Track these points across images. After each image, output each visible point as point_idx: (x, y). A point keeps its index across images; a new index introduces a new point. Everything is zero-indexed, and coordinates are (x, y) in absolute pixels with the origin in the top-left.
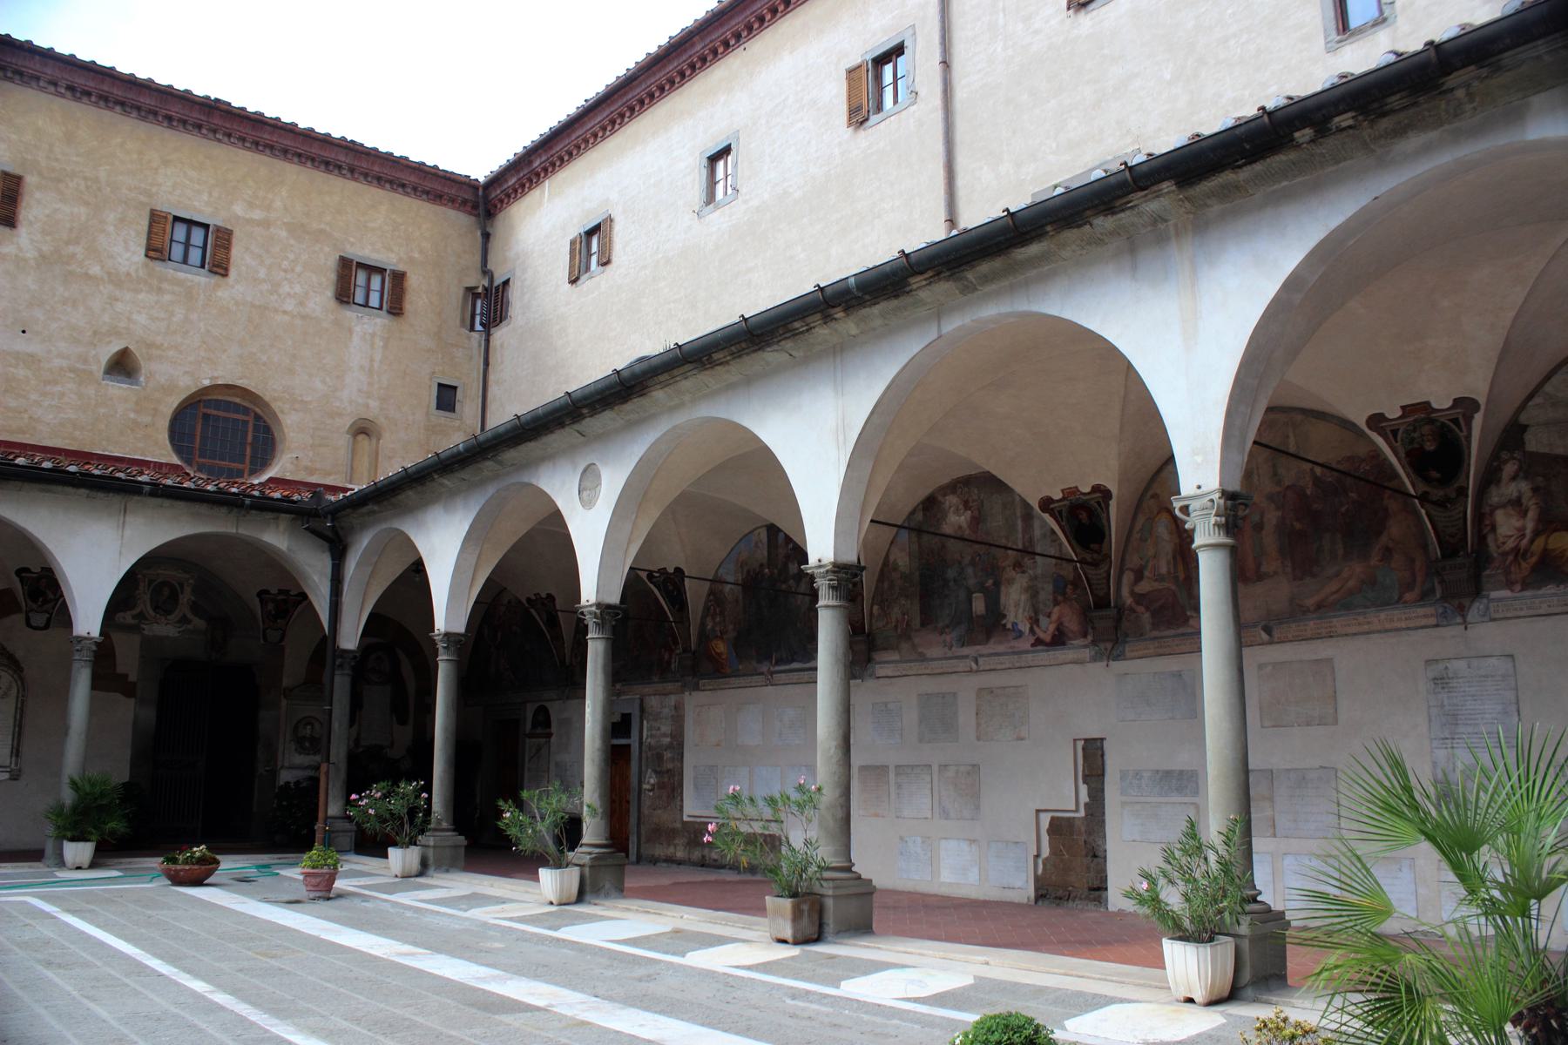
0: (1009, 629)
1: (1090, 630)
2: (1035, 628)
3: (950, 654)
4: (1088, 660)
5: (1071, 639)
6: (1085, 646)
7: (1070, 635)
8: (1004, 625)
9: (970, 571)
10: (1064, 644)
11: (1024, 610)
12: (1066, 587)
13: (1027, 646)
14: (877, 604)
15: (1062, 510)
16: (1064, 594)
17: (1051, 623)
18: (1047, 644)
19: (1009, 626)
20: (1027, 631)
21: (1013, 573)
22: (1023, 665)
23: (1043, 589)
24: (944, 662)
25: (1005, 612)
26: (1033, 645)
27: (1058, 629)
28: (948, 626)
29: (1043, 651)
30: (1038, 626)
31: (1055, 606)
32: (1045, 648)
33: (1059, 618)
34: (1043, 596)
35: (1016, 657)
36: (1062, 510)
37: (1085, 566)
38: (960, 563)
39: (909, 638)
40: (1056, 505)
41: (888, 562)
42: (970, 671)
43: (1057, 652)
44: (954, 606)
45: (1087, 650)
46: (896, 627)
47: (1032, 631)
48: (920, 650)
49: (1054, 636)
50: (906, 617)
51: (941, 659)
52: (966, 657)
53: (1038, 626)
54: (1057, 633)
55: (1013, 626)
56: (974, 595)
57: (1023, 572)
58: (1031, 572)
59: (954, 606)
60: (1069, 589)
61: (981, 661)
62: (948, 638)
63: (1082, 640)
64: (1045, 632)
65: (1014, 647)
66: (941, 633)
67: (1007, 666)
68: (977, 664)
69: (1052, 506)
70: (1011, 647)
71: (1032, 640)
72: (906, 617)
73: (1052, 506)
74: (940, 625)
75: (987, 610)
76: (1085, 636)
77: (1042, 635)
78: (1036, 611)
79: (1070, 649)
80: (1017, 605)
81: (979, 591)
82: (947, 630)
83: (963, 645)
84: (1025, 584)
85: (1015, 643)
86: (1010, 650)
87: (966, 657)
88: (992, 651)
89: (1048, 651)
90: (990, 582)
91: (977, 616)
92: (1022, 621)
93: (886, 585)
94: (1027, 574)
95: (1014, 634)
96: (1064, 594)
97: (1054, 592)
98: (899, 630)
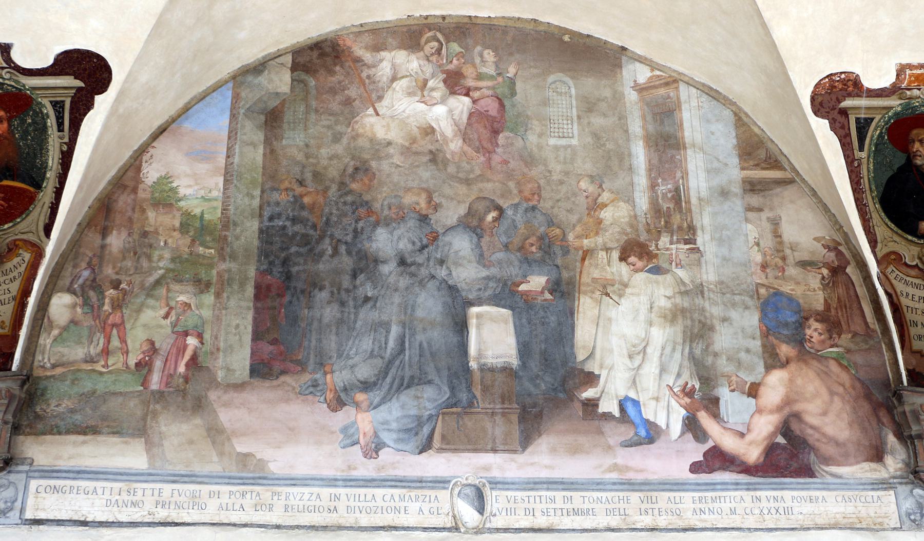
0: (607, 416)
1: (891, 439)
2: (704, 419)
3: (366, 469)
4: (894, 522)
5: (827, 460)
6: (884, 485)
7: (828, 450)
8: (591, 405)
9: (462, 244)
10: (807, 471)
11: (663, 370)
12: (802, 324)
13: (679, 469)
14: (70, 290)
15: (869, 121)
16: (799, 341)
17: (759, 411)
18: (748, 470)
19: (609, 406)
20: (676, 428)
21: (624, 269)
22: (662, 522)
23: (725, 320)
24: (342, 491)
25: (593, 367)
26: (695, 468)
27: (785, 429)
28: (366, 386)
29: (737, 485)
30: (716, 416)
31: (769, 368)
32: (743, 478)
33: (788, 401)
34: (723, 339)
35: (635, 497)
36: (869, 121)
37: (893, 272)
38: (424, 219)
39: (199, 405)
40: (863, 102)
41: (138, 180)
42: (456, 529)
43: (787, 494)
44: (395, 330)
45: (889, 497)
46: (144, 366)
47: (692, 426)
48: (241, 447)
49: (771, 450)
50: (192, 341)
51: (331, 482)
52: (440, 483)
53: (716, 416)
54: (781, 440)
55: (622, 409)
56: (474, 310)
57: (657, 270)
58: (681, 273)
59: (395, 330)
60: (814, 331)
61: (495, 500)
62: (365, 422)
63: (866, 465)
64: (742, 435)
65: (627, 469)
66: (338, 404)
67: (602, 521)
68: (481, 510)
69: (848, 103)
70: (615, 468)
71: (696, 452)
72: (192, 341)
73: (848, 103)
74: (339, 378)
75: (524, 350)
76: (877, 455)
77: (729, 443)
78: (707, 378)
79: (826, 487)
80: (638, 352)
81: (496, 300)
82: (360, 397)
83: (425, 447)
84: (663, 303)
85: (625, 457)
86: (614, 476)
87: (440, 483)
88: (544, 474)
89: (749, 487)
90: (536, 282)
91: (483, 368)
92: (657, 399)
93: (116, 241)
94: (668, 277)
95: (628, 433)
96: (799, 341)
97: (766, 334)
98: (155, 381)
